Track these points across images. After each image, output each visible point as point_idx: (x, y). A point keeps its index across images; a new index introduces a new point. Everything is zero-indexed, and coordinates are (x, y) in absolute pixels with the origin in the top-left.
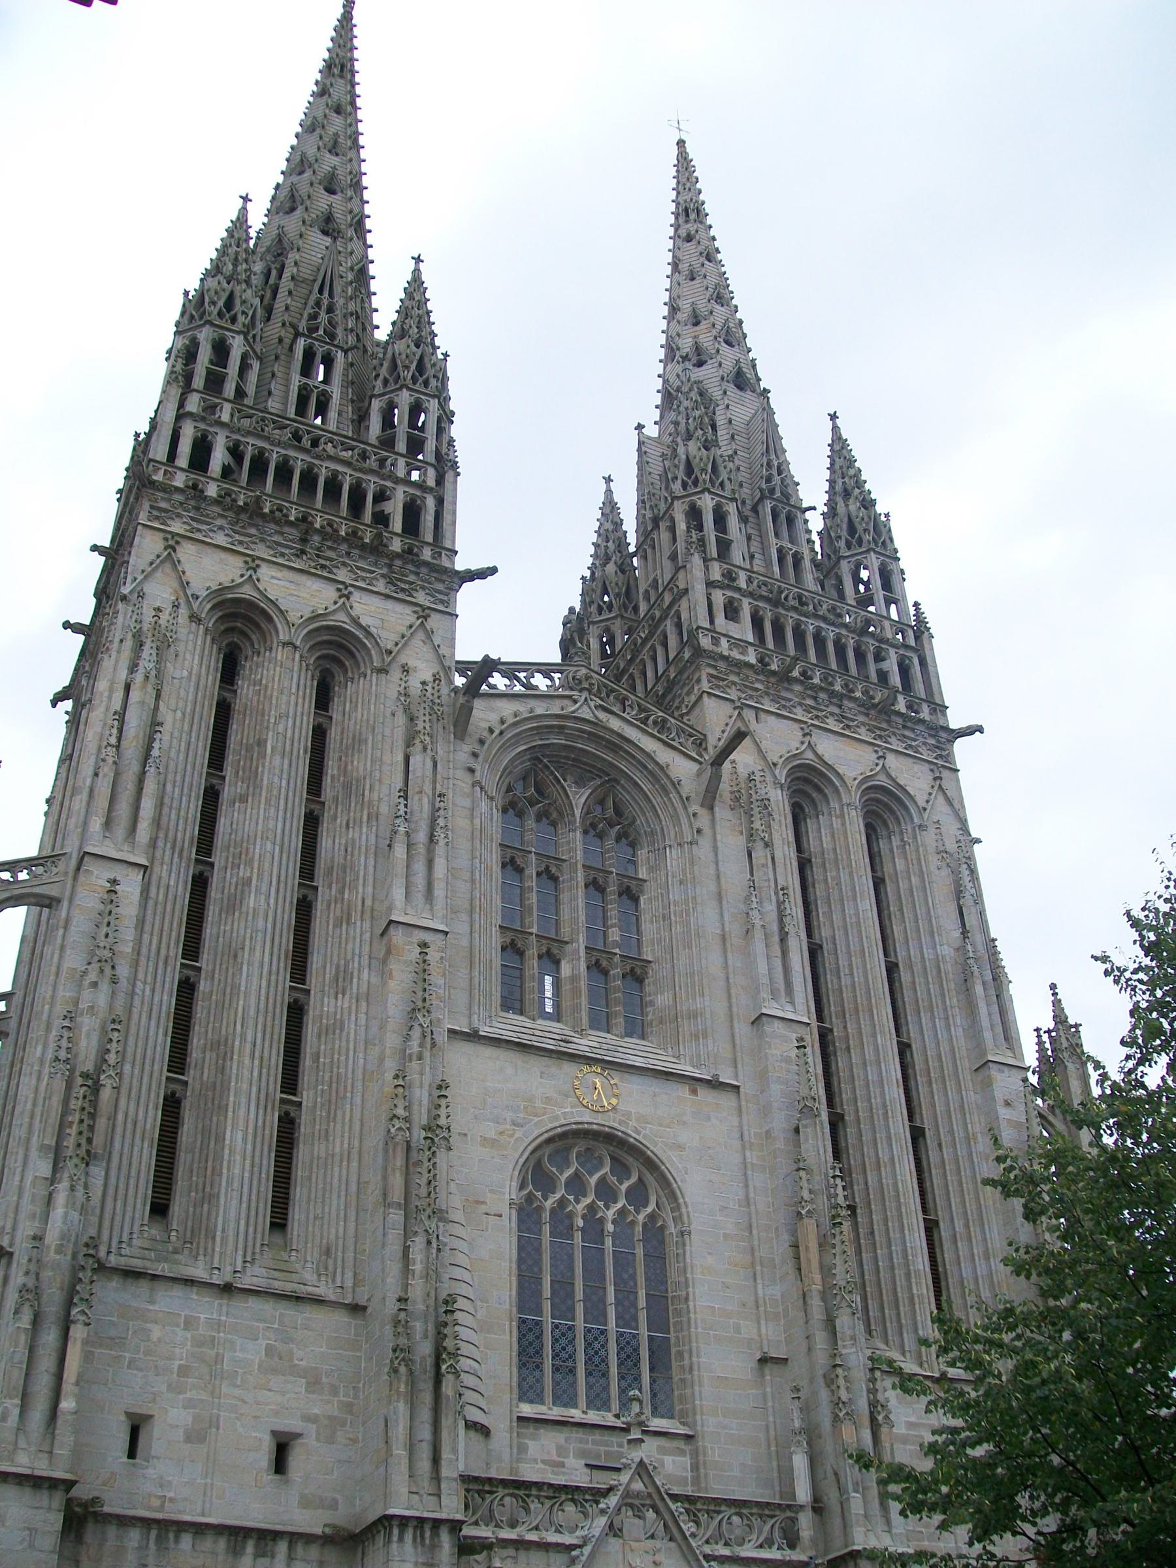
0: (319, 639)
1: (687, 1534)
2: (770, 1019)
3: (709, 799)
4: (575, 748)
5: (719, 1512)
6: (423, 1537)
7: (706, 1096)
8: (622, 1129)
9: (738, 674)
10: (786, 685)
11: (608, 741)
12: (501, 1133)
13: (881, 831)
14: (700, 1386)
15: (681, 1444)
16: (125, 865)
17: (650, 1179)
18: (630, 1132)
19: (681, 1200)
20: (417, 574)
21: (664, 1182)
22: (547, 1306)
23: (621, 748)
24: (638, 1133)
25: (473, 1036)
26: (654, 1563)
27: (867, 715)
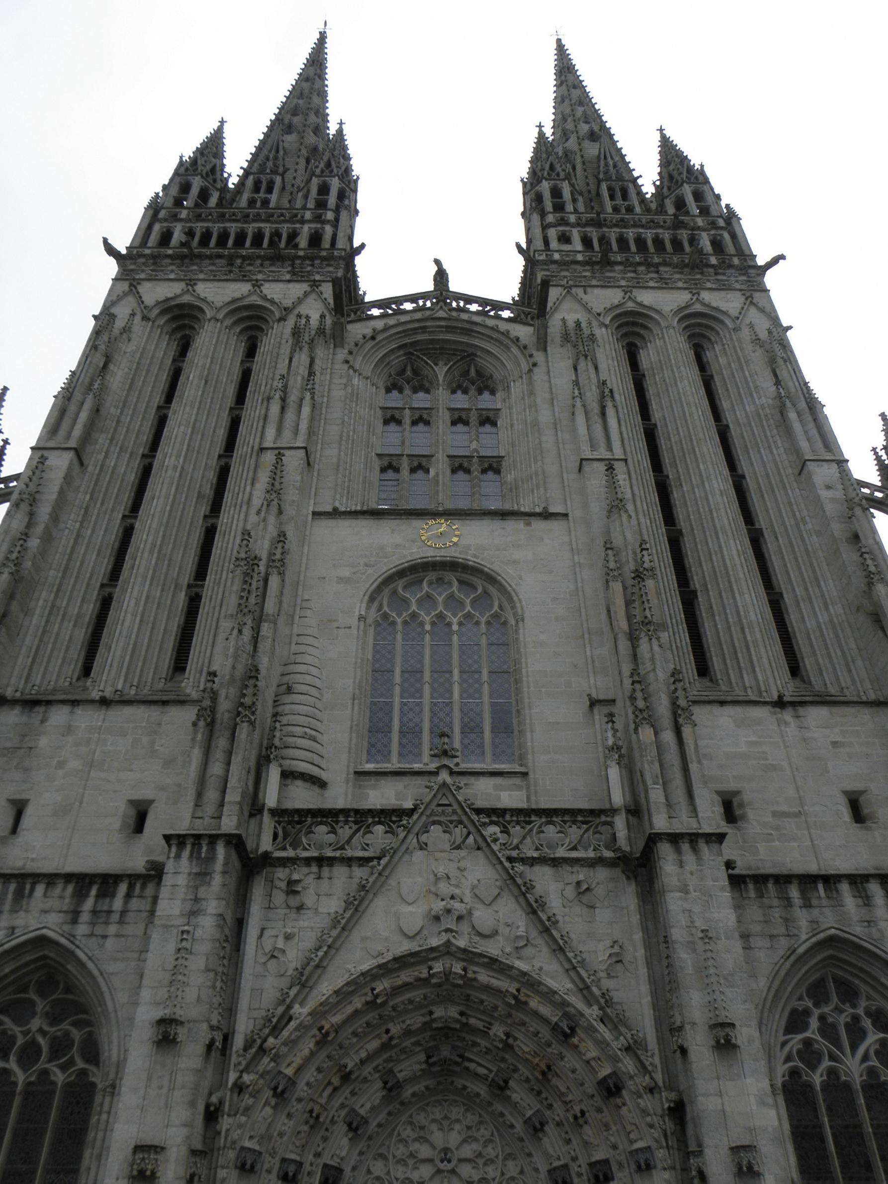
0: (240, 316)
1: (489, 840)
2: (588, 462)
3: (542, 343)
4: (439, 340)
5: (529, 823)
6: (199, 852)
7: (539, 525)
8: (462, 556)
9: (567, 270)
10: (609, 268)
11: (462, 328)
12: (354, 573)
13: (706, 344)
14: (532, 731)
15: (518, 781)
16: (60, 451)
17: (492, 590)
18: (469, 558)
19: (515, 598)
20: (312, 265)
21: (502, 589)
22: (397, 690)
23: (472, 331)
24: (477, 557)
25: (335, 514)
26: (459, 868)
27: (682, 273)
